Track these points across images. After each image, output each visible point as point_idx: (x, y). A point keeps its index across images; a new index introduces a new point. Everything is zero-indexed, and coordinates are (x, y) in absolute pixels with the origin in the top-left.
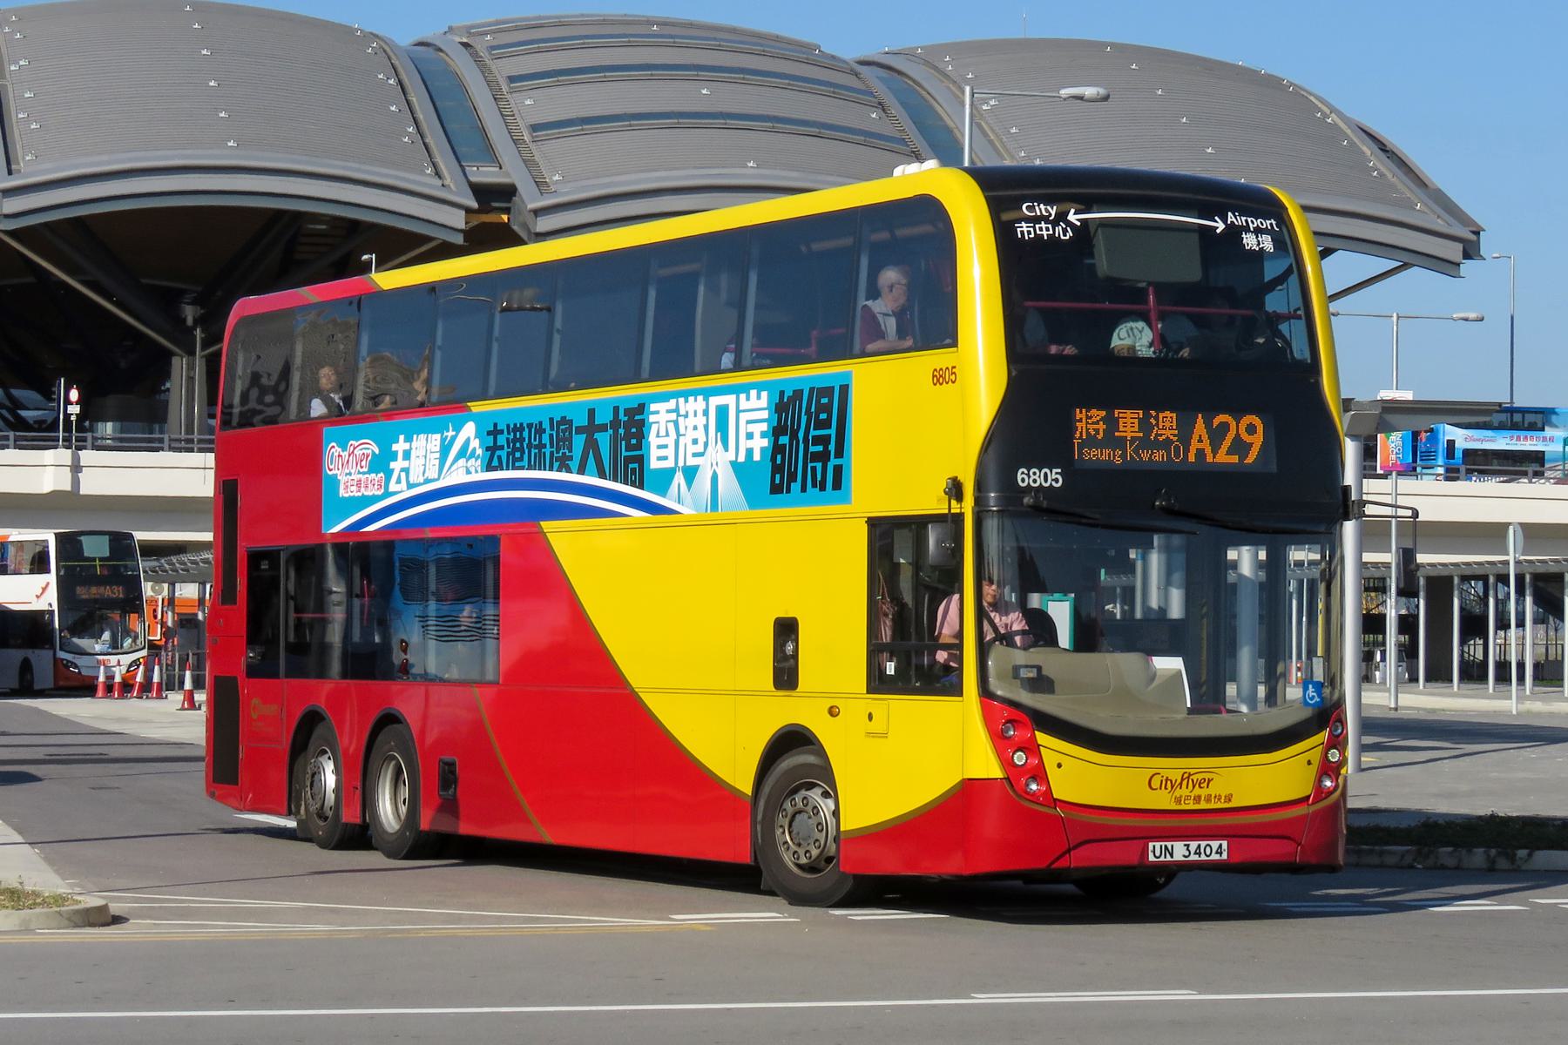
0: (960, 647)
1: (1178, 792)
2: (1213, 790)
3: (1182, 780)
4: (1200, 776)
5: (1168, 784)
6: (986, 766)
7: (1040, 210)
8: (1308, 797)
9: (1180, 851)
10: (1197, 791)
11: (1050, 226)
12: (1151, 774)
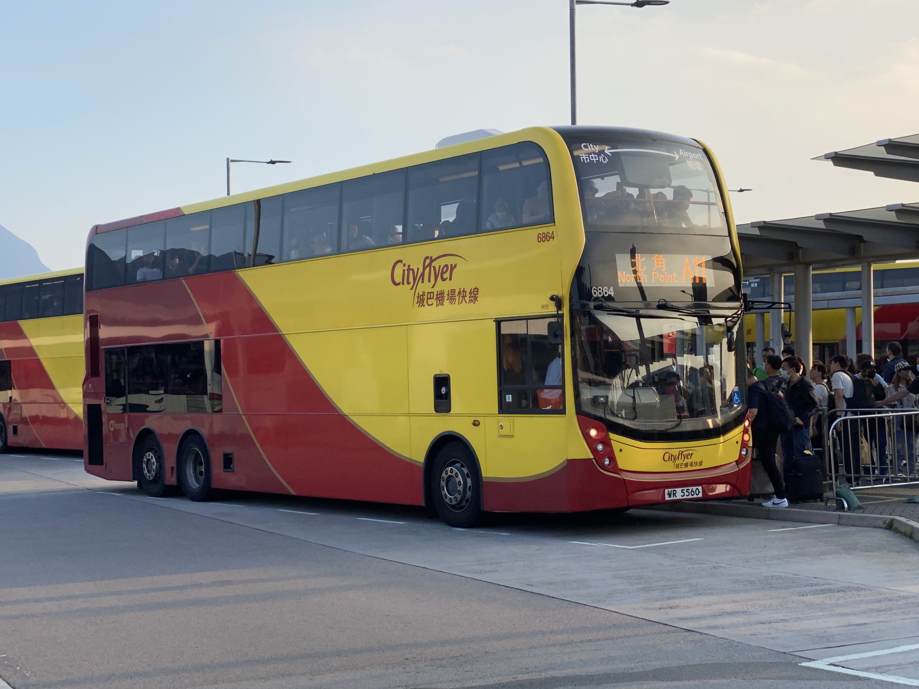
0: (562, 387)
1: (678, 462)
2: (693, 459)
3: (679, 455)
4: (687, 453)
5: (672, 458)
6: (583, 452)
7: (590, 147)
8: (737, 461)
9: (679, 494)
10: (686, 461)
11: (596, 156)
12: (663, 455)
